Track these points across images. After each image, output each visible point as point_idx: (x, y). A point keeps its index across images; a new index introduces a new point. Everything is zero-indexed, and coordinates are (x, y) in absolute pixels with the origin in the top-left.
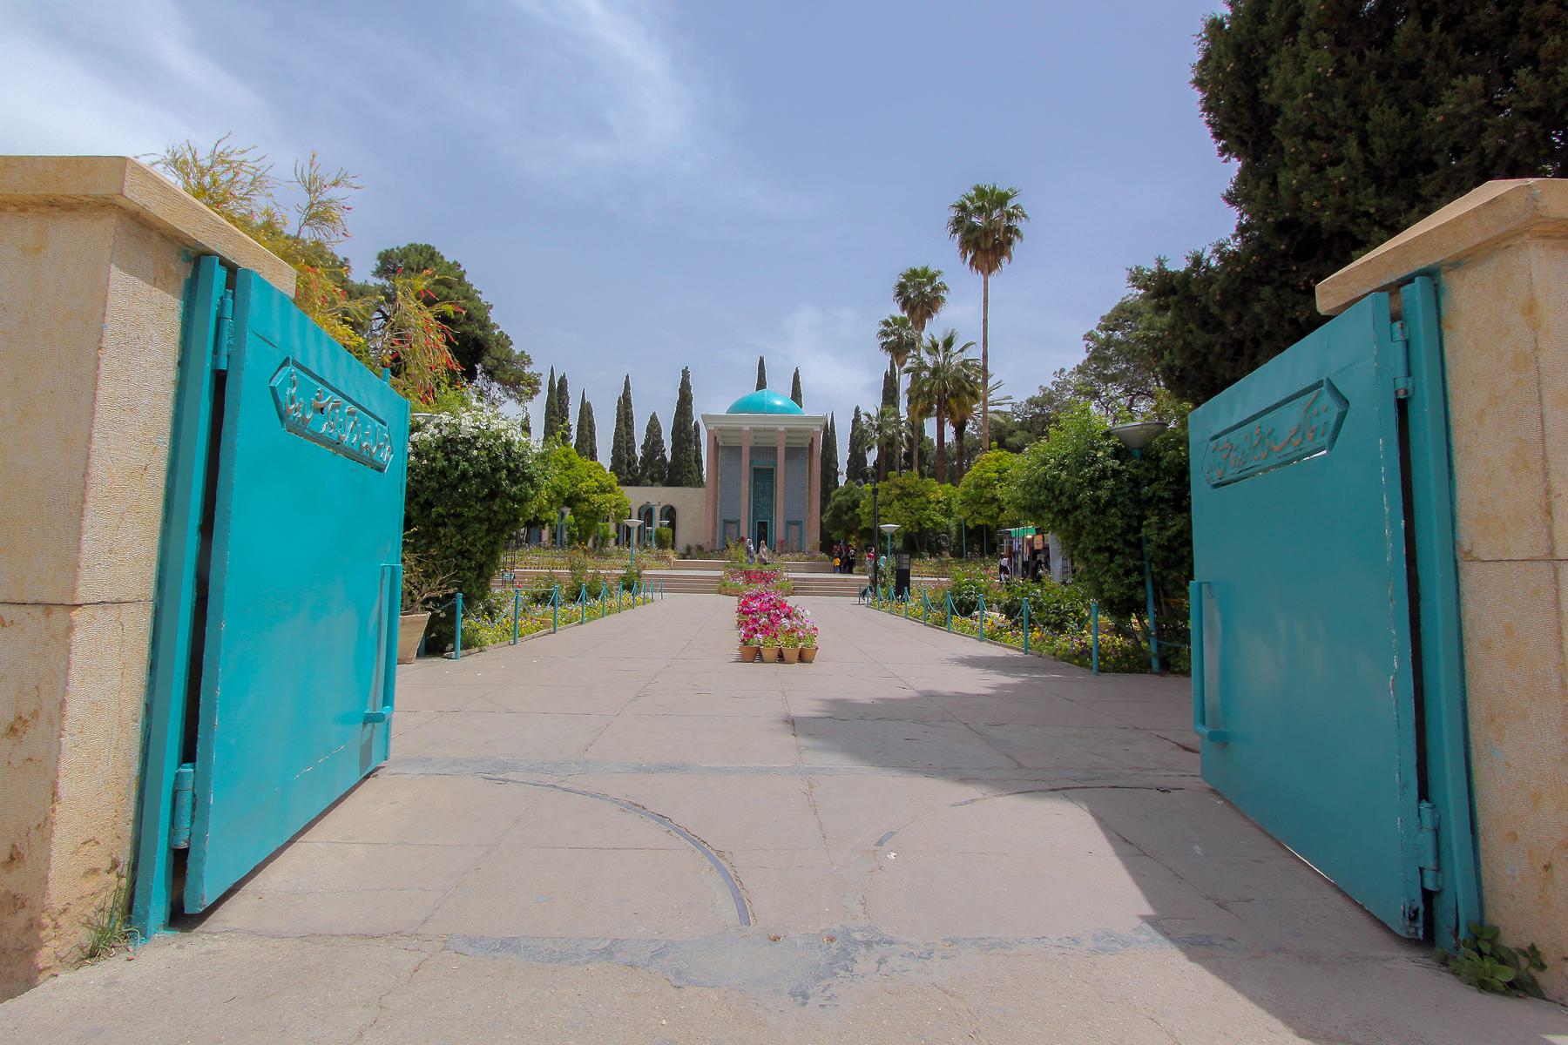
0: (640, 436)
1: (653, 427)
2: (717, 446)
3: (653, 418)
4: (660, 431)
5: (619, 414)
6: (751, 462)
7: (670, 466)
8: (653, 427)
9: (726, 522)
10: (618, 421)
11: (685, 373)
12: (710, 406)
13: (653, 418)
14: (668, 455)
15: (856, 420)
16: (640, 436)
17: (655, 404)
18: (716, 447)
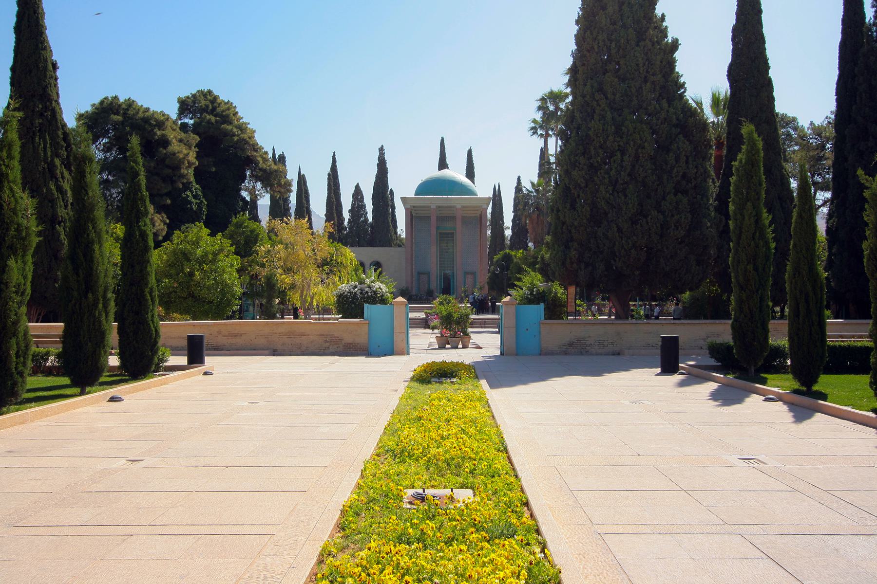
0: (347, 202)
1: (358, 193)
2: (412, 216)
3: (357, 187)
4: (362, 197)
5: (329, 185)
6: (438, 228)
7: (372, 225)
8: (358, 193)
9: (419, 273)
10: (329, 189)
11: (381, 149)
12: (403, 187)
13: (357, 187)
14: (370, 217)
15: (519, 189)
16: (347, 202)
17: (358, 177)
18: (412, 217)
